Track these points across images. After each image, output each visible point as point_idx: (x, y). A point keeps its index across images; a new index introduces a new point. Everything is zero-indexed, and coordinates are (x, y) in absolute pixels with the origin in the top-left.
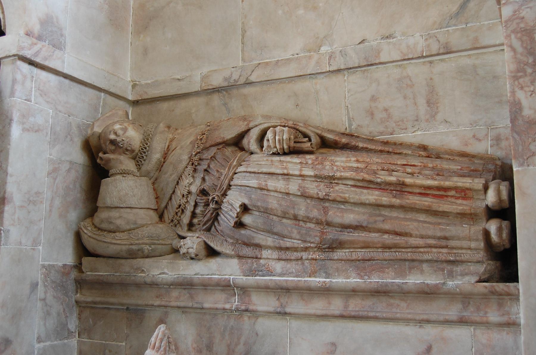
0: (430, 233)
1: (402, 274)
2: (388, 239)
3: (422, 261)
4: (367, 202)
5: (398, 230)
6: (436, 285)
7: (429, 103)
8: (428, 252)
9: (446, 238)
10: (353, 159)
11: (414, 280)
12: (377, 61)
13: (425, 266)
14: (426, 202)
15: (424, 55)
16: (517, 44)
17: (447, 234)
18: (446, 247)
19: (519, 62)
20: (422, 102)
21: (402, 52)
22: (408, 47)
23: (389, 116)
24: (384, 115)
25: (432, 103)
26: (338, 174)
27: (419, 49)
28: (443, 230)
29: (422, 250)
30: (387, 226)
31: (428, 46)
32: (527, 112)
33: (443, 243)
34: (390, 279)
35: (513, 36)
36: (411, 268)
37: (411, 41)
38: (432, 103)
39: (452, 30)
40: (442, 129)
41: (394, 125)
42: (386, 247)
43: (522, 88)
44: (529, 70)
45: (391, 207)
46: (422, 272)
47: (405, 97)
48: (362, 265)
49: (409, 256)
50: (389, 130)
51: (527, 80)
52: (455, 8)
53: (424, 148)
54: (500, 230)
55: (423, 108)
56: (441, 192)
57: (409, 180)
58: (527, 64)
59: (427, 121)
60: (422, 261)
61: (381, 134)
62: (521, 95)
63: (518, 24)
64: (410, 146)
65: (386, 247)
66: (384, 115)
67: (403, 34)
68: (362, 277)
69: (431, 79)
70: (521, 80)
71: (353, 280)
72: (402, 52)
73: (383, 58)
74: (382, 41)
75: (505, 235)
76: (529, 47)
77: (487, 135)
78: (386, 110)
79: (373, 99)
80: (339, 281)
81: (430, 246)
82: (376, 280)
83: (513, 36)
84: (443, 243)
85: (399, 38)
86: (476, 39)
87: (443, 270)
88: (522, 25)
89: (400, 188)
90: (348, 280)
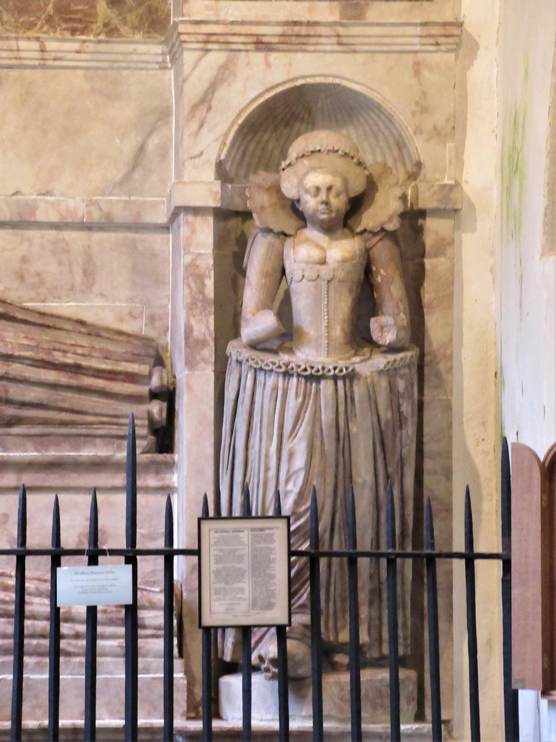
0: (104, 411)
1: (77, 448)
2: (65, 416)
3: (95, 436)
4: (47, 382)
5: (76, 408)
6: (108, 458)
7: (86, 273)
8: (101, 428)
9: (116, 416)
10: (23, 335)
11: (87, 452)
12: (32, 219)
13: (98, 441)
14: (100, 383)
15: (85, 221)
16: (193, 285)
17: (118, 413)
18: (117, 424)
19: (193, 298)
20: (78, 270)
21: (60, 214)
22: (68, 210)
23: (42, 282)
24: (36, 280)
25: (89, 273)
26: (17, 353)
27: (80, 214)
28: (114, 409)
29: (96, 426)
30: (66, 405)
31: (89, 213)
32: (196, 334)
33: (115, 420)
34: (68, 453)
35: (190, 278)
36: (85, 443)
37: (71, 203)
38: (89, 273)
39: (115, 200)
40: (99, 302)
41: (47, 292)
42: (63, 424)
43: (194, 316)
44: (199, 304)
45: (68, 388)
46: (95, 446)
47: (60, 263)
48: (40, 440)
49: (84, 431)
50: (41, 297)
51: (198, 311)
52: (119, 176)
53: (82, 323)
54: (161, 410)
55: (78, 279)
56: (112, 375)
57: (84, 363)
58: (198, 300)
59: (83, 291)
60: (95, 436)
61: (32, 300)
62: (193, 321)
63: (194, 270)
64: (68, 319)
65: (63, 424)
66: (36, 280)
67: (63, 194)
68: (38, 451)
69: (89, 247)
70: (194, 311)
71: (30, 454)
72: (60, 214)
73: (40, 216)
74: (39, 197)
75: (164, 415)
76: (200, 287)
77: (142, 313)
78: (38, 274)
79: (24, 260)
80: (17, 455)
81: (103, 423)
82: (52, 453)
83: (190, 278)
84: (115, 420)
85: (57, 198)
86: (138, 215)
87: (113, 444)
88: (197, 271)
89: (77, 369)
90: (26, 454)
